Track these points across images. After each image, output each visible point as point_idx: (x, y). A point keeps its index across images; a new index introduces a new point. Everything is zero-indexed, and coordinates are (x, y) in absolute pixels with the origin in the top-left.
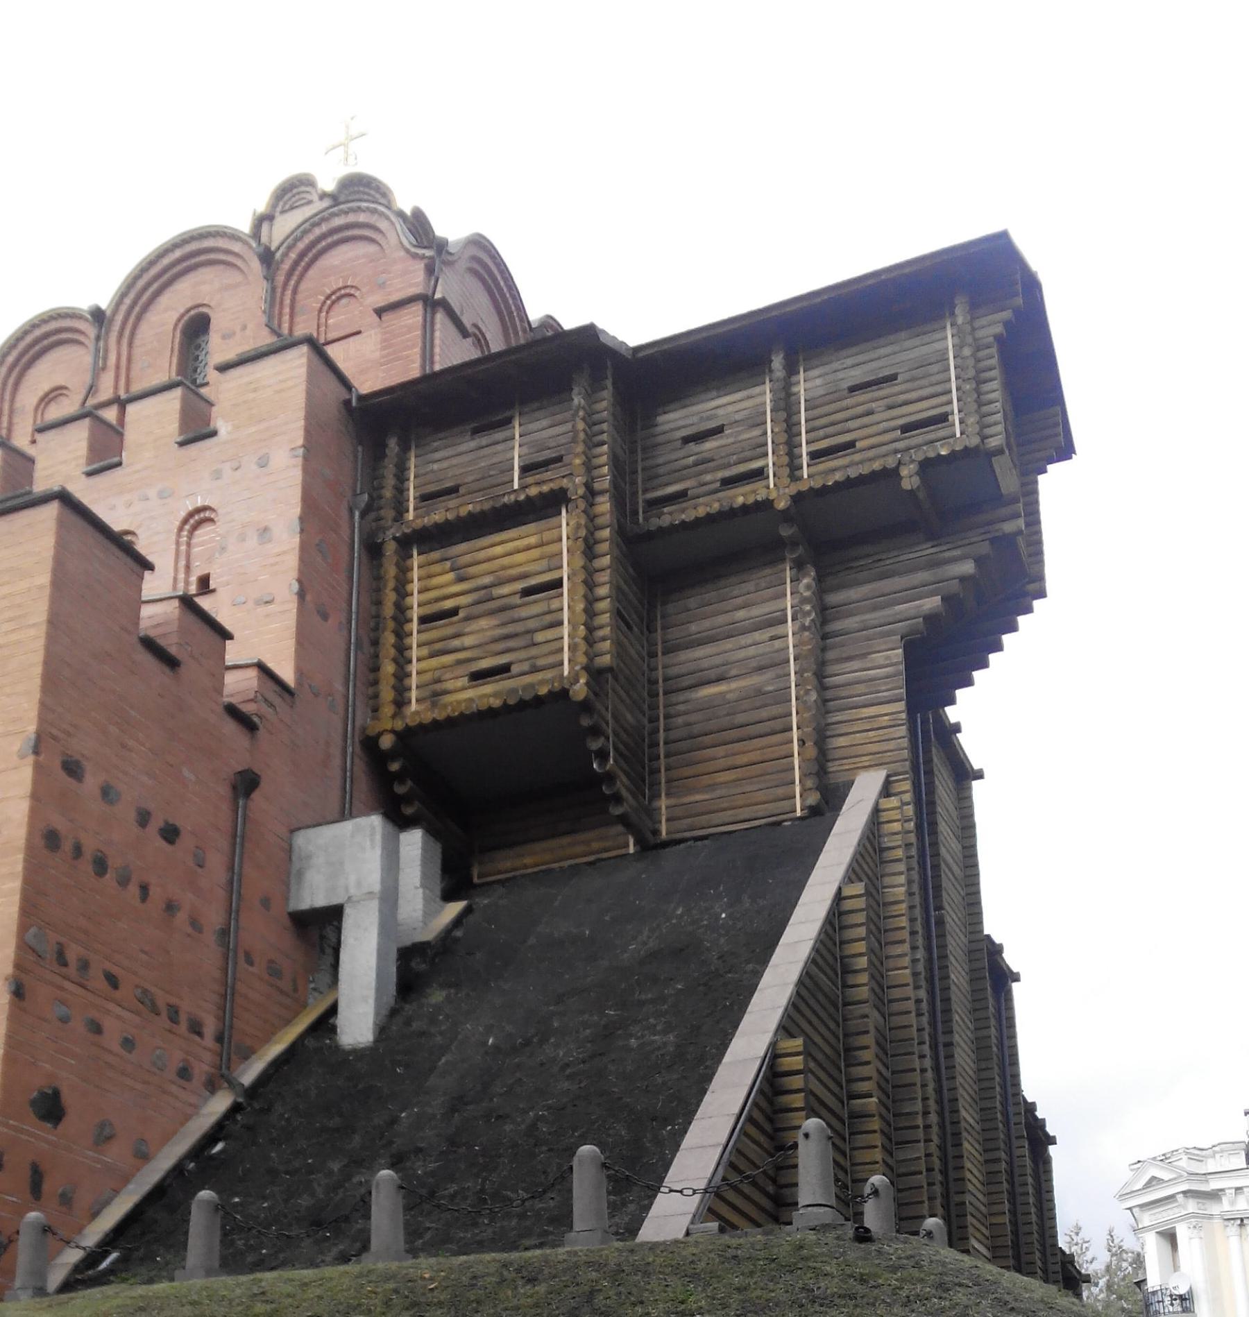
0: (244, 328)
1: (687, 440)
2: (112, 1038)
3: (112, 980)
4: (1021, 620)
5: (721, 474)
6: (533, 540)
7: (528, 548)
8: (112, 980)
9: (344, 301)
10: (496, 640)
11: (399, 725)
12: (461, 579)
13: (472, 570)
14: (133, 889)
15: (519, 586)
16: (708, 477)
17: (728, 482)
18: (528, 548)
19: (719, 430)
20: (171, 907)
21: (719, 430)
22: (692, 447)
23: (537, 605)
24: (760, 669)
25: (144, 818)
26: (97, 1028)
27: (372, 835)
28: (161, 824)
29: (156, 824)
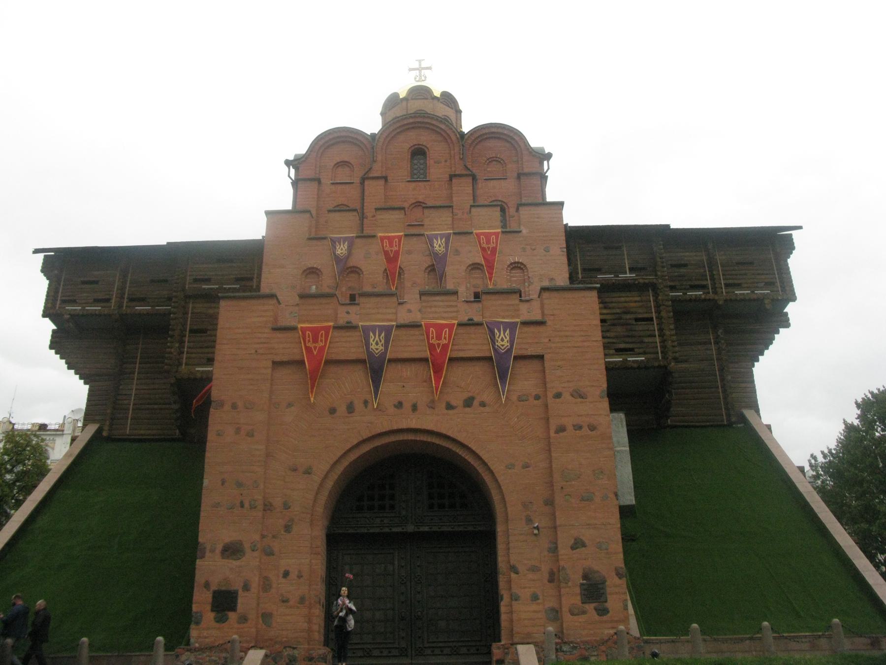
0: (446, 161)
1: (672, 266)
5: (689, 283)
6: (638, 299)
7: (635, 302)
9: (494, 163)
10: (624, 336)
12: (605, 308)
13: (611, 305)
15: (633, 316)
18: (635, 302)
19: (685, 265)
21: (685, 265)
23: (641, 327)
27: (621, 421)
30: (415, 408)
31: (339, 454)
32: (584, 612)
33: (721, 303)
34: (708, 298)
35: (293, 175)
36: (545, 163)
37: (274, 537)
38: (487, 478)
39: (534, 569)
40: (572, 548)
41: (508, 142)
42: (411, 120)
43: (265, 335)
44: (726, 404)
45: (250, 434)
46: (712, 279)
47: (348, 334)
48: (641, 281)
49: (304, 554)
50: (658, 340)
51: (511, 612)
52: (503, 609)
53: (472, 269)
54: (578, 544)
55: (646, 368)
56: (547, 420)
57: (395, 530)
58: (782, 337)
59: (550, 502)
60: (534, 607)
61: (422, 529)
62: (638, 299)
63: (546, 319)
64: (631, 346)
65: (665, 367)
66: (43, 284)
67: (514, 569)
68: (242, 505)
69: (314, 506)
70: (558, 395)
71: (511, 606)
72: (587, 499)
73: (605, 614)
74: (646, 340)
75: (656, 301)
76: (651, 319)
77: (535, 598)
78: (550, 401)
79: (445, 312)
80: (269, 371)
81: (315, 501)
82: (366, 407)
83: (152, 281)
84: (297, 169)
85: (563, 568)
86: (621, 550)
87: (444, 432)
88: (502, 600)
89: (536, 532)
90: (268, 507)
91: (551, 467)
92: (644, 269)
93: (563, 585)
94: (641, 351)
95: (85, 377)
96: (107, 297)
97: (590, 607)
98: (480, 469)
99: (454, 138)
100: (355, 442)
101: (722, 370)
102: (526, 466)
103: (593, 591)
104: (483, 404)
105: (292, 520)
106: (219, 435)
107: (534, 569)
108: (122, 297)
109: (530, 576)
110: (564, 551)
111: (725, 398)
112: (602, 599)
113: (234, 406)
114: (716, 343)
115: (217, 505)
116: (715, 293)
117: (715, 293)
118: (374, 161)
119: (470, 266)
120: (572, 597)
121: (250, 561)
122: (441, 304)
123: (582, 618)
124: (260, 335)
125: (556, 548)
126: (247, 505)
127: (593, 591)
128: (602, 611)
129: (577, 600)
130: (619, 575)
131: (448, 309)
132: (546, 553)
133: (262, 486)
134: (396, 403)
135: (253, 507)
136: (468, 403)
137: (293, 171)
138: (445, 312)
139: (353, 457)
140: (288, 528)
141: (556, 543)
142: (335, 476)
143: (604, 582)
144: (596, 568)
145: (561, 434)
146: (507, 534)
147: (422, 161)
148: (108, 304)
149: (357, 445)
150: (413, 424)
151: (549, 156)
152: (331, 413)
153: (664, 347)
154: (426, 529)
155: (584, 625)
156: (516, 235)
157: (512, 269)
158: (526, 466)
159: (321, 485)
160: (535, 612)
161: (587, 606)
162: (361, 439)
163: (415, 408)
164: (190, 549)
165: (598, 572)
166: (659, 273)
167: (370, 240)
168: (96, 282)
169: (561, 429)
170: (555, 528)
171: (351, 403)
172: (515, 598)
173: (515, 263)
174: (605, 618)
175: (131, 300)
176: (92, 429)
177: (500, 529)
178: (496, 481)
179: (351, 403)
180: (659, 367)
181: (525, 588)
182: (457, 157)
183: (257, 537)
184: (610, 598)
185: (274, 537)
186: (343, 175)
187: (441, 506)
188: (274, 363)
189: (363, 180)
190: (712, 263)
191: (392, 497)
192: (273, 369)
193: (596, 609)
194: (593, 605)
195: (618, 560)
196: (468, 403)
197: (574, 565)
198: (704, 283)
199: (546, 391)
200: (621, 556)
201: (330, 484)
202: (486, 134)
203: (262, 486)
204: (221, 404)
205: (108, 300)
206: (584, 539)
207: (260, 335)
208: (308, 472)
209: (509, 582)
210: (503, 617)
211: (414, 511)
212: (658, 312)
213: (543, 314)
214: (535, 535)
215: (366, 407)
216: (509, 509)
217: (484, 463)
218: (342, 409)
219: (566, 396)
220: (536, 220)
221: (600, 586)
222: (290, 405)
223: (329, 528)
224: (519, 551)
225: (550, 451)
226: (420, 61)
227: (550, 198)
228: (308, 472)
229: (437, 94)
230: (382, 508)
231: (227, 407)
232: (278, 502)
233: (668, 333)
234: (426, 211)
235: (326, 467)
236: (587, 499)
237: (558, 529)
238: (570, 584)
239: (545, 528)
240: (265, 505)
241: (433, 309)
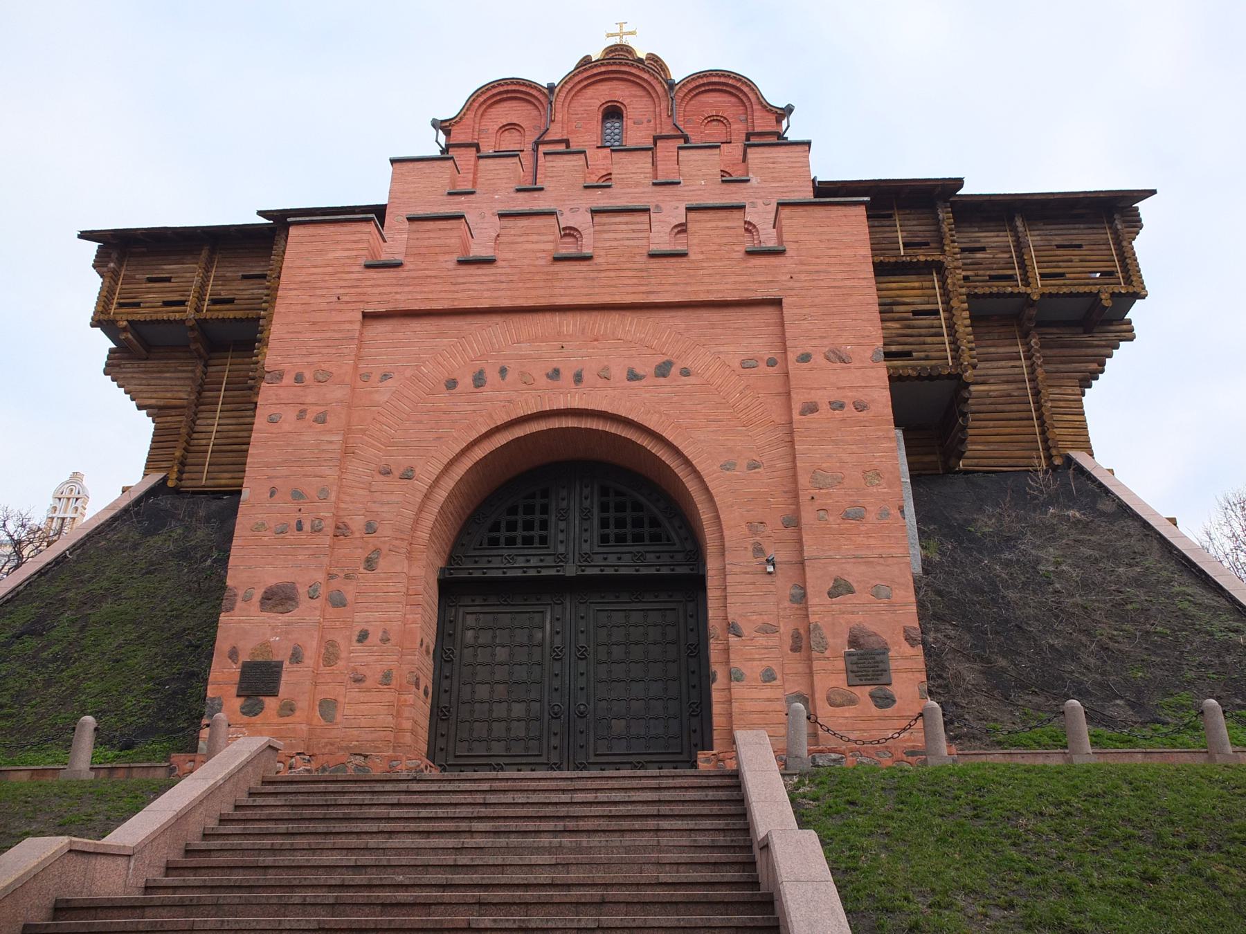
0: (649, 121)
4: (1094, 382)
6: (916, 284)
16: (981, 272)
17: (992, 278)
21: (983, 249)
24: (1007, 382)
30: (578, 378)
31: (458, 450)
32: (852, 702)
33: (1035, 298)
34: (1016, 290)
35: (443, 142)
36: (785, 123)
37: (347, 577)
38: (691, 485)
39: (767, 630)
40: (831, 594)
42: (603, 69)
43: (354, 276)
44: (1045, 441)
45: (321, 419)
46: (1023, 265)
47: (480, 272)
48: (922, 258)
49: (397, 607)
50: (946, 339)
51: (730, 701)
52: (716, 696)
53: (679, 232)
54: (840, 588)
55: (930, 378)
56: (788, 394)
57: (545, 572)
58: (1121, 360)
59: (793, 522)
60: (767, 693)
61: (589, 571)
62: (916, 284)
63: (787, 246)
64: (907, 348)
65: (958, 377)
66: (94, 282)
67: (733, 629)
68: (300, 527)
69: (414, 529)
71: (729, 689)
72: (854, 516)
73: (887, 706)
74: (929, 340)
75: (943, 286)
76: (936, 312)
77: (769, 676)
78: (793, 366)
79: (628, 239)
80: (357, 326)
81: (417, 521)
82: (503, 378)
83: (245, 277)
84: (447, 133)
85: (816, 627)
86: (913, 599)
87: (623, 413)
88: (714, 680)
89: (770, 569)
90: (341, 531)
91: (794, 468)
92: (927, 244)
93: (814, 654)
94: (922, 355)
95: (156, 411)
96: (183, 298)
97: (863, 692)
98: (681, 472)
99: (659, 88)
100: (484, 430)
101: (1037, 393)
102: (754, 466)
103: (867, 664)
104: (686, 373)
105: (378, 550)
106: (272, 421)
107: (767, 630)
108: (200, 298)
109: (762, 640)
110: (817, 599)
111: (1043, 433)
112: (884, 680)
113: (299, 379)
114: (1028, 358)
115: (259, 528)
116: (1027, 285)
117: (1027, 285)
118: (552, 121)
119: (676, 226)
120: (831, 675)
121: (307, 613)
122: (624, 227)
123: (848, 711)
124: (346, 276)
125: (804, 595)
126: (307, 526)
127: (867, 664)
128: (885, 701)
129: (840, 681)
130: (910, 640)
131: (635, 235)
132: (787, 604)
133: (333, 497)
134: (550, 371)
135: (316, 530)
136: (663, 370)
137: (442, 138)
138: (628, 239)
139: (479, 453)
140: (370, 564)
141: (804, 588)
142: (449, 483)
143: (885, 650)
144: (871, 627)
145: (811, 416)
146: (723, 572)
147: (617, 125)
148: (182, 308)
150: (576, 403)
151: (789, 110)
152: (448, 388)
153: (956, 350)
154: (596, 571)
155: (855, 721)
156: (742, 185)
158: (754, 466)
159: (427, 497)
160: (769, 700)
161: (857, 691)
162: (493, 426)
163: (578, 378)
164: (212, 593)
165: (875, 634)
166: (947, 248)
167: (536, 194)
168: (168, 280)
170: (802, 562)
171: (481, 372)
172: (734, 676)
174: (888, 711)
175: (214, 302)
176: (156, 477)
177: (712, 565)
178: (706, 489)
179: (481, 372)
180: (949, 376)
181: (753, 660)
182: (664, 115)
183: (320, 577)
184: (895, 678)
185: (347, 577)
186: (510, 142)
187: (621, 539)
188: (366, 316)
189: (537, 144)
190: (1020, 247)
191: (544, 525)
192: (363, 324)
193: (872, 696)
194: (868, 689)
195: (909, 616)
196: (663, 370)
197: (834, 622)
198: (1010, 272)
199: (785, 352)
200: (914, 609)
201: (442, 495)
202: (704, 85)
203: (333, 497)
204: (280, 376)
205: (182, 303)
206: (850, 580)
207: (346, 276)
208: (408, 476)
209: (727, 650)
210: (717, 709)
211: (576, 546)
212: (946, 302)
213: (781, 241)
214: (770, 573)
215: (503, 378)
216: (726, 533)
217: (687, 462)
218: (466, 382)
221: (878, 658)
222: (386, 376)
223: (442, 570)
224: (743, 600)
225: (792, 442)
226: (621, 25)
227: (791, 136)
229: (641, 54)
230: (528, 541)
231: (288, 380)
232: (357, 524)
233: (961, 329)
234: (614, 155)
235: (437, 468)
236: (854, 516)
237: (807, 563)
238: (827, 653)
239: (785, 563)
240: (338, 528)
241: (612, 235)
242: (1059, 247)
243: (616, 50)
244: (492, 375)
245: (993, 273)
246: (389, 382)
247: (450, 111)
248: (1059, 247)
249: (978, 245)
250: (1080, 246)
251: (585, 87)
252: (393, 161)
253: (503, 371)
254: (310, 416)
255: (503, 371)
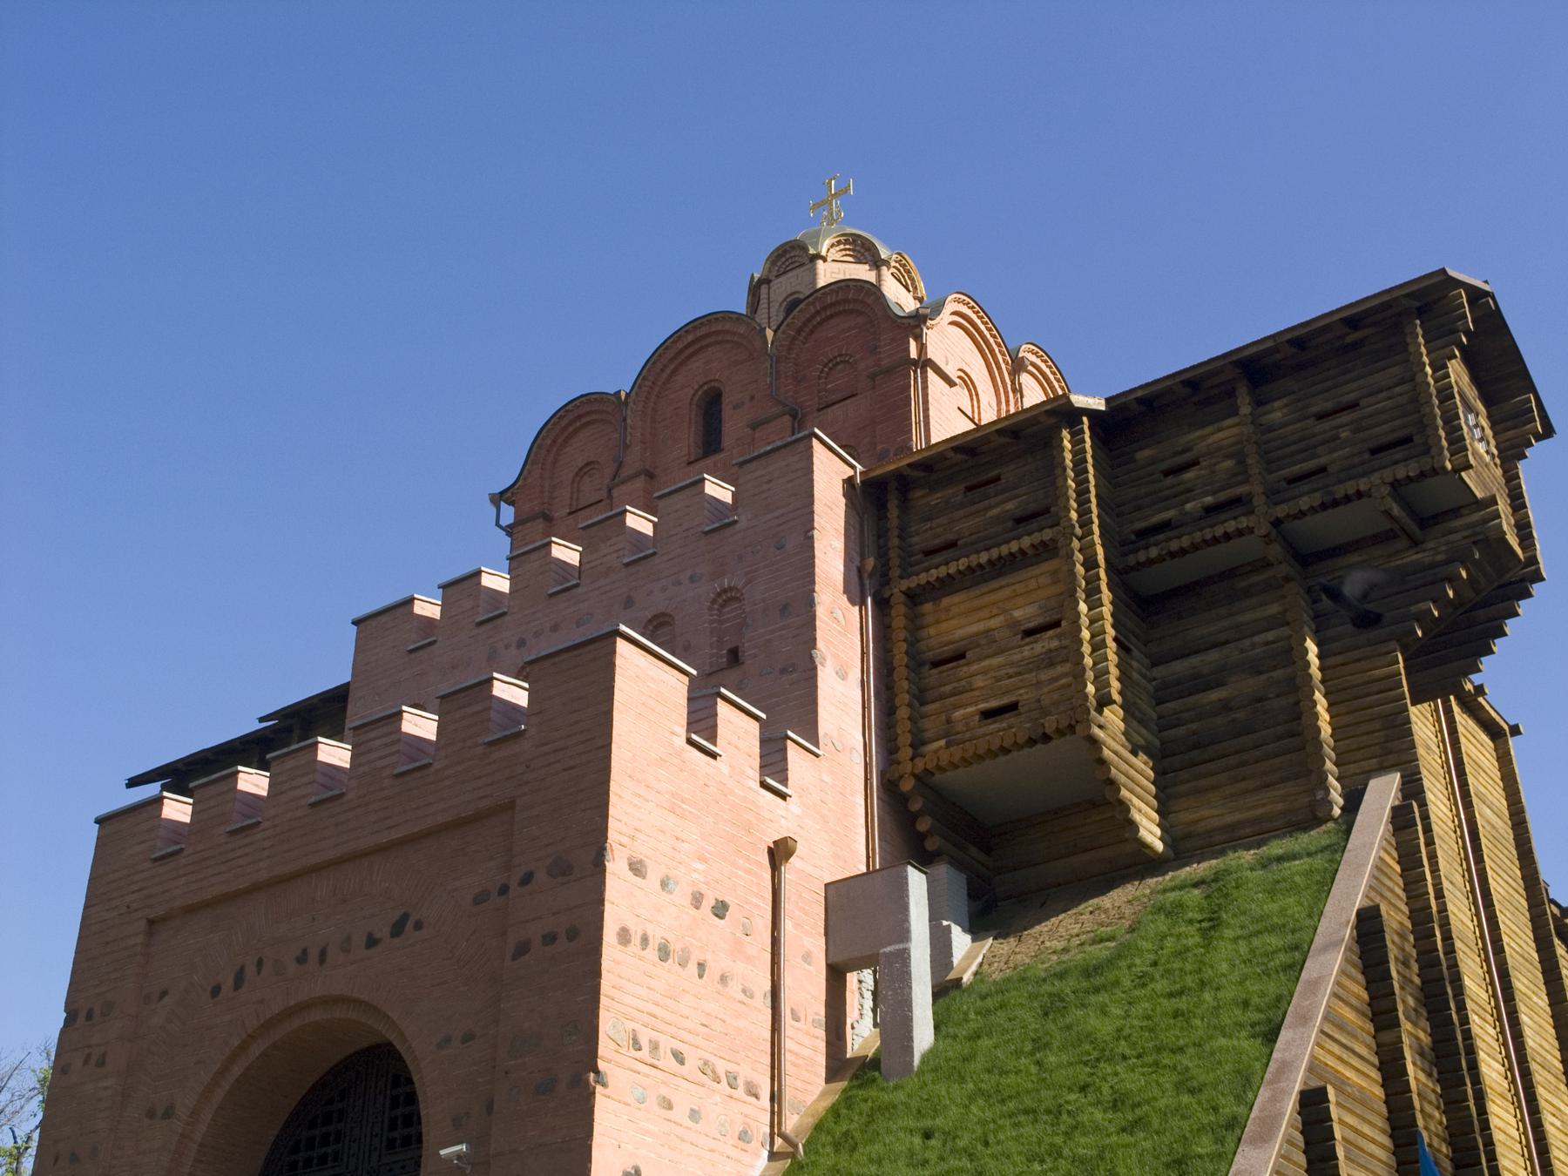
1: (1167, 473)
2: (680, 1113)
3: (679, 1058)
8: (679, 1058)
11: (920, 764)
14: (692, 968)
17: (1210, 510)
20: (723, 979)
22: (1170, 480)
25: (697, 900)
26: (669, 1106)
28: (713, 903)
29: (708, 903)
41: (851, 312)
42: (690, 338)
70: (527, 879)
100: (236, 1042)
104: (418, 926)
122: (378, 743)
136: (398, 929)
149: (244, 1047)
157: (722, 606)
158: (468, 1038)
167: (499, 621)
169: (522, 949)
171: (242, 969)
173: (725, 591)
219: (541, 877)
220: (766, 487)
222: (164, 994)
228: (168, 1114)
242: (1320, 417)
243: (785, 252)
244: (250, 970)
245: (1209, 500)
246: (166, 1000)
247: (506, 476)
248: (1320, 417)
249: (1187, 457)
250: (1353, 406)
251: (674, 372)
252: (355, 623)
253: (260, 963)
254: (93, 1061)
255: (260, 963)
